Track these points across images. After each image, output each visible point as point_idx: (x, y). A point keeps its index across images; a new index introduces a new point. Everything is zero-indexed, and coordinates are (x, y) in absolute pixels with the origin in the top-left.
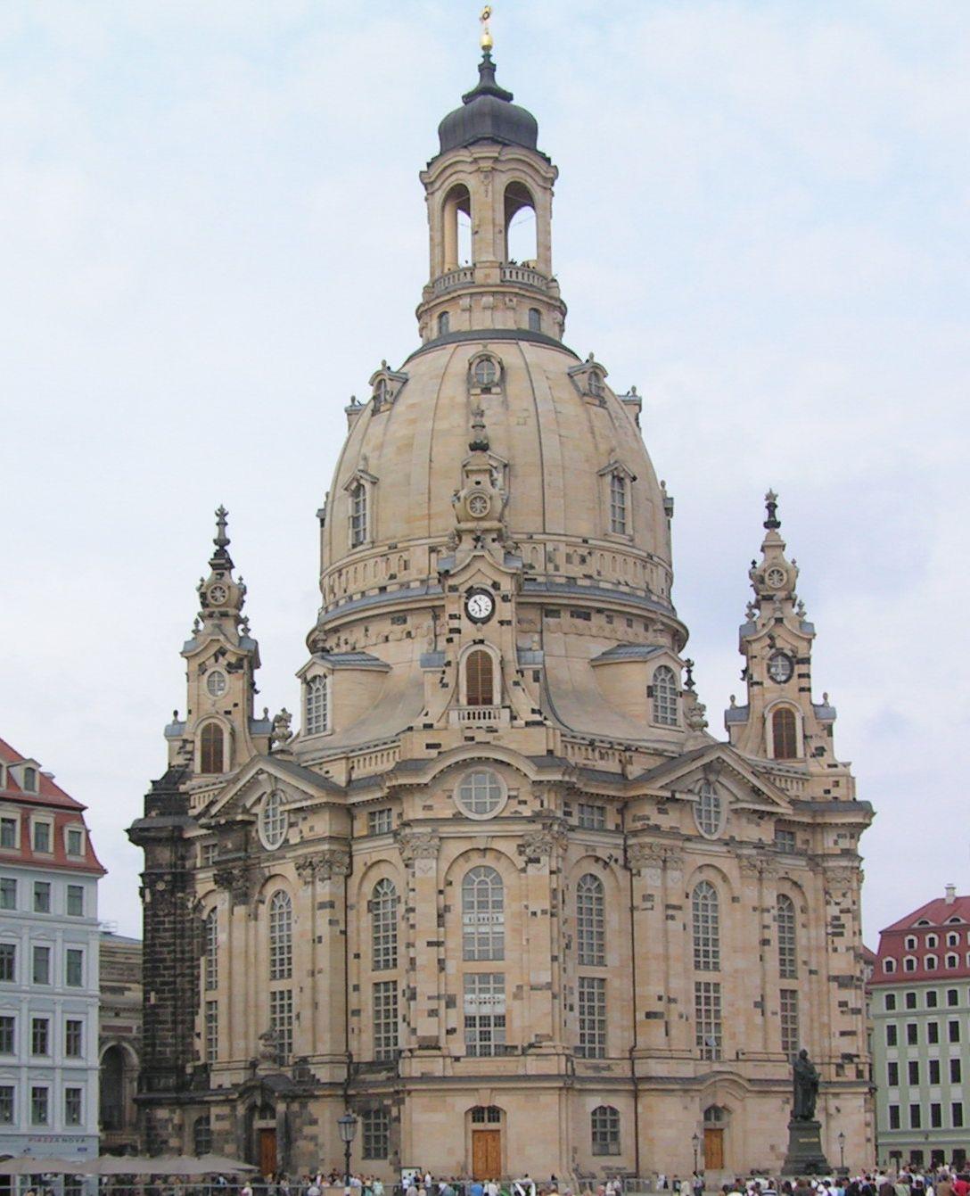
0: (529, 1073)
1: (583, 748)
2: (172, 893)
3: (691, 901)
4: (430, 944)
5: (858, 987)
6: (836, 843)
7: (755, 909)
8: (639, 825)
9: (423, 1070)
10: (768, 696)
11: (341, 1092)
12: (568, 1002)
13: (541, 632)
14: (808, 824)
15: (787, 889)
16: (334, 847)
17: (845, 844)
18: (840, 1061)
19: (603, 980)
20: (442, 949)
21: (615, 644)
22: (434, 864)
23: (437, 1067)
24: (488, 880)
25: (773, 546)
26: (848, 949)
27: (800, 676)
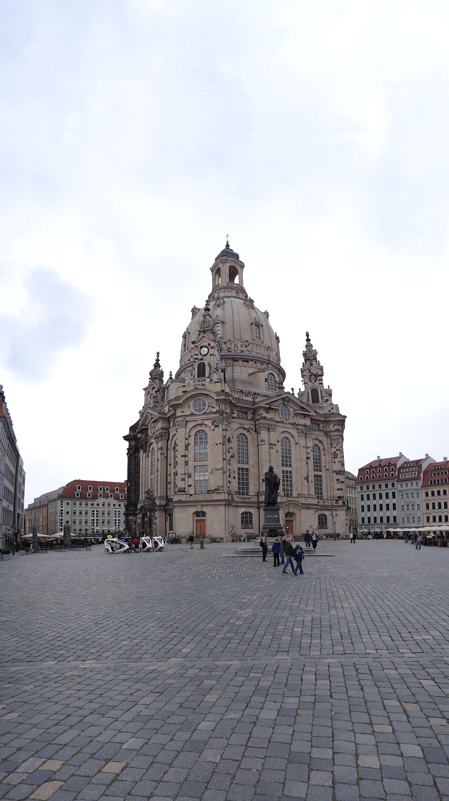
0: (214, 499)
1: (239, 393)
2: (135, 454)
3: (280, 443)
4: (182, 456)
5: (342, 474)
7: (304, 447)
8: (259, 417)
10: (309, 386)
11: (163, 508)
15: (317, 443)
16: (163, 431)
19: (247, 469)
20: (187, 458)
21: (257, 370)
22: (184, 430)
23: (183, 498)
25: (309, 346)
27: (319, 380)
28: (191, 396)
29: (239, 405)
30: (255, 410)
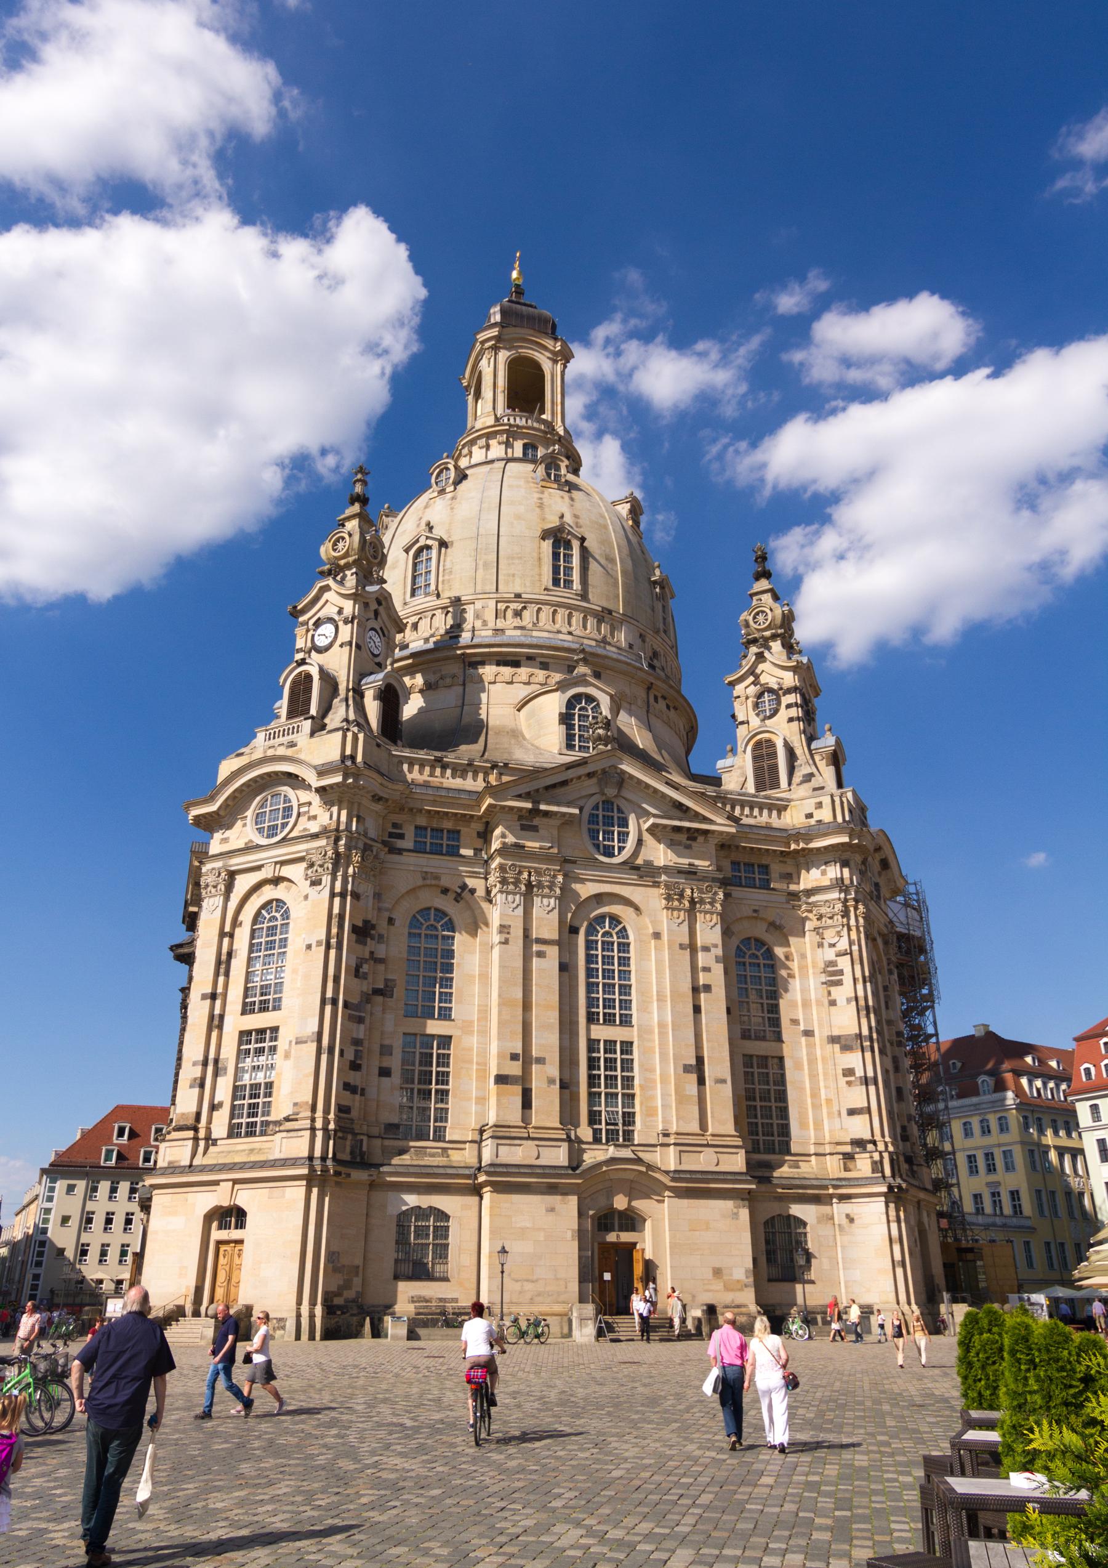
0: (277, 1155)
4: (204, 997)
6: (824, 873)
7: (682, 947)
9: (172, 1159)
12: (372, 1064)
13: (464, 685)
14: (782, 852)
17: (833, 871)
18: (848, 1149)
20: (218, 1003)
24: (278, 915)
26: (849, 1001)
27: (788, 706)
28: (246, 784)
29: (418, 805)
30: (487, 823)
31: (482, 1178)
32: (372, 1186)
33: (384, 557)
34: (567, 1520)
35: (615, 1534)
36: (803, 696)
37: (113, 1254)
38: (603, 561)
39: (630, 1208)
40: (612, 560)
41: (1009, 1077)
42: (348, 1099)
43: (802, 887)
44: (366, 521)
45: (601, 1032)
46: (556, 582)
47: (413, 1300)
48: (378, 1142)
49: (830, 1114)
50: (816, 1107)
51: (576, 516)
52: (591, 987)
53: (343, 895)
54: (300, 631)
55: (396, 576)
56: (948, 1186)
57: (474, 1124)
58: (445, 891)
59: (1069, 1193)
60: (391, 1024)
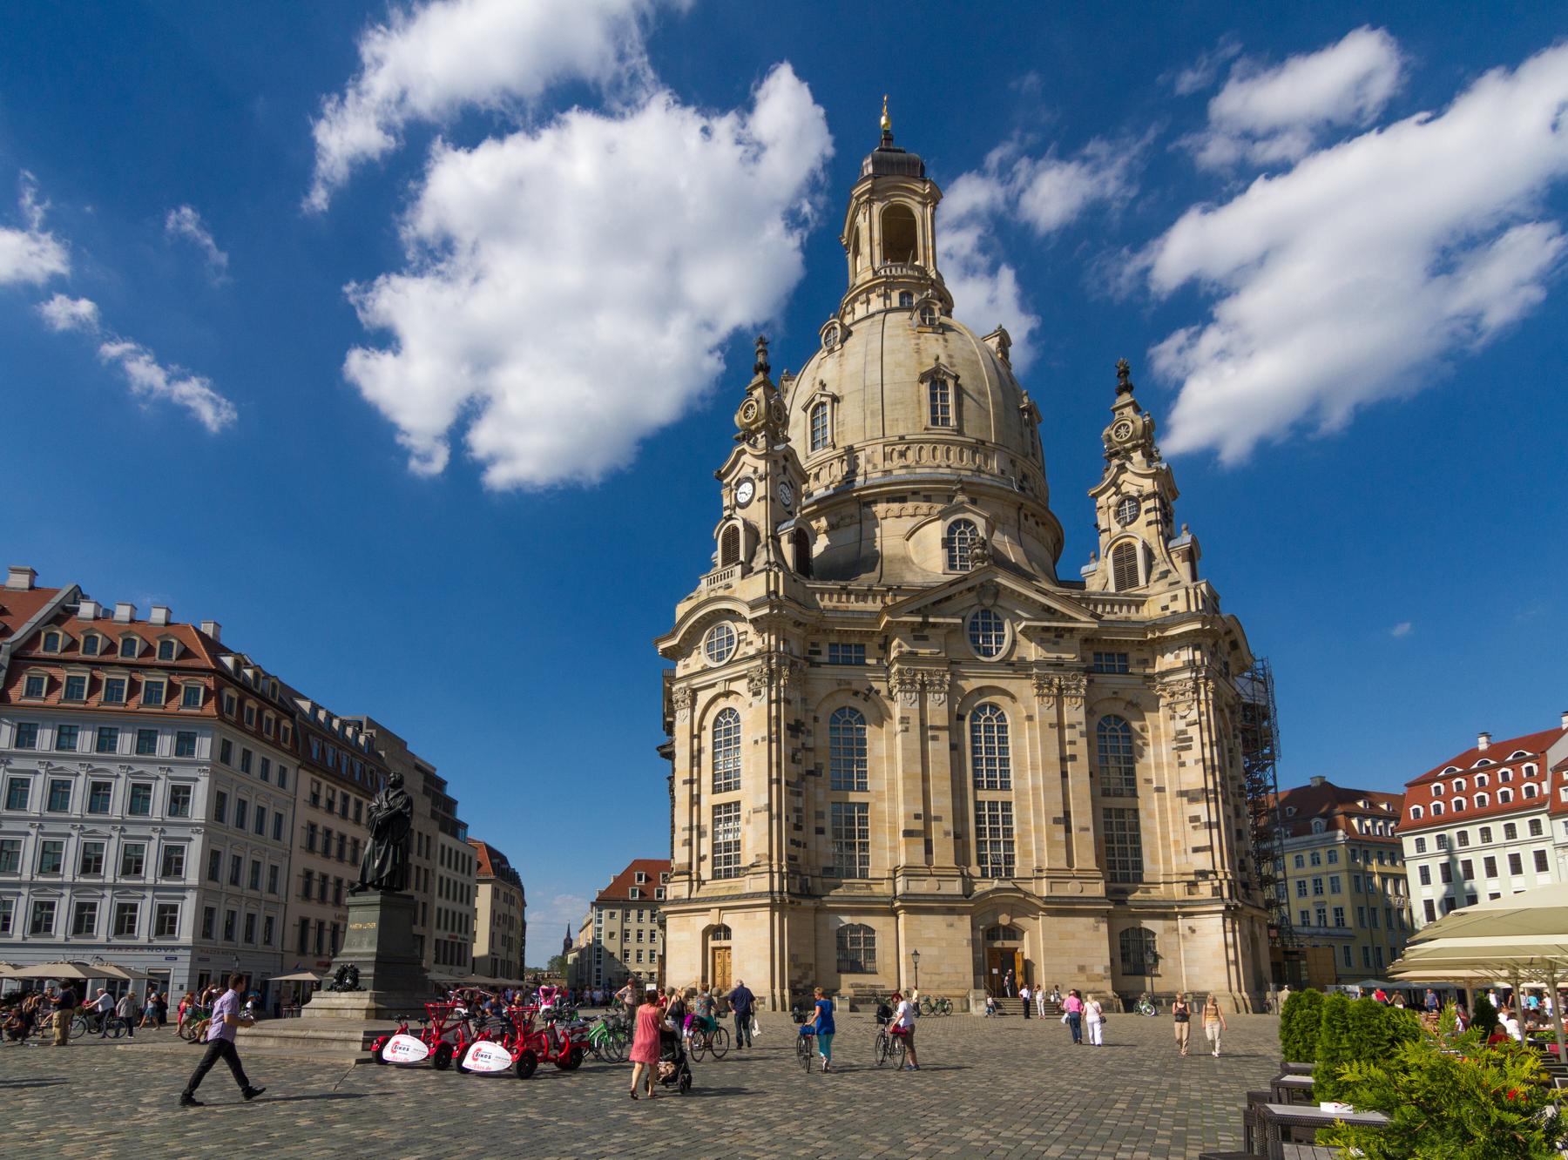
0: (748, 891)
4: (685, 782)
18: (1192, 878)
31: (897, 904)
32: (817, 910)
33: (787, 417)
34: (971, 1125)
35: (1008, 1134)
36: (1161, 500)
37: (645, 956)
38: (975, 396)
39: (1012, 924)
40: (983, 394)
41: (1341, 818)
42: (795, 851)
43: (1157, 670)
44: (771, 387)
45: (985, 796)
46: (934, 421)
47: (852, 986)
48: (818, 880)
49: (1177, 853)
50: (1166, 846)
51: (950, 356)
52: (976, 762)
53: (778, 701)
54: (725, 492)
55: (798, 433)
56: (1279, 905)
57: (889, 866)
58: (856, 693)
59: (1389, 909)
60: (822, 795)
